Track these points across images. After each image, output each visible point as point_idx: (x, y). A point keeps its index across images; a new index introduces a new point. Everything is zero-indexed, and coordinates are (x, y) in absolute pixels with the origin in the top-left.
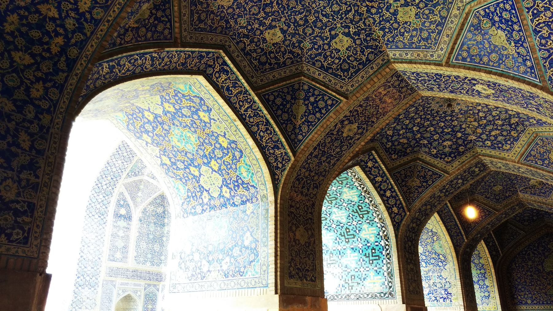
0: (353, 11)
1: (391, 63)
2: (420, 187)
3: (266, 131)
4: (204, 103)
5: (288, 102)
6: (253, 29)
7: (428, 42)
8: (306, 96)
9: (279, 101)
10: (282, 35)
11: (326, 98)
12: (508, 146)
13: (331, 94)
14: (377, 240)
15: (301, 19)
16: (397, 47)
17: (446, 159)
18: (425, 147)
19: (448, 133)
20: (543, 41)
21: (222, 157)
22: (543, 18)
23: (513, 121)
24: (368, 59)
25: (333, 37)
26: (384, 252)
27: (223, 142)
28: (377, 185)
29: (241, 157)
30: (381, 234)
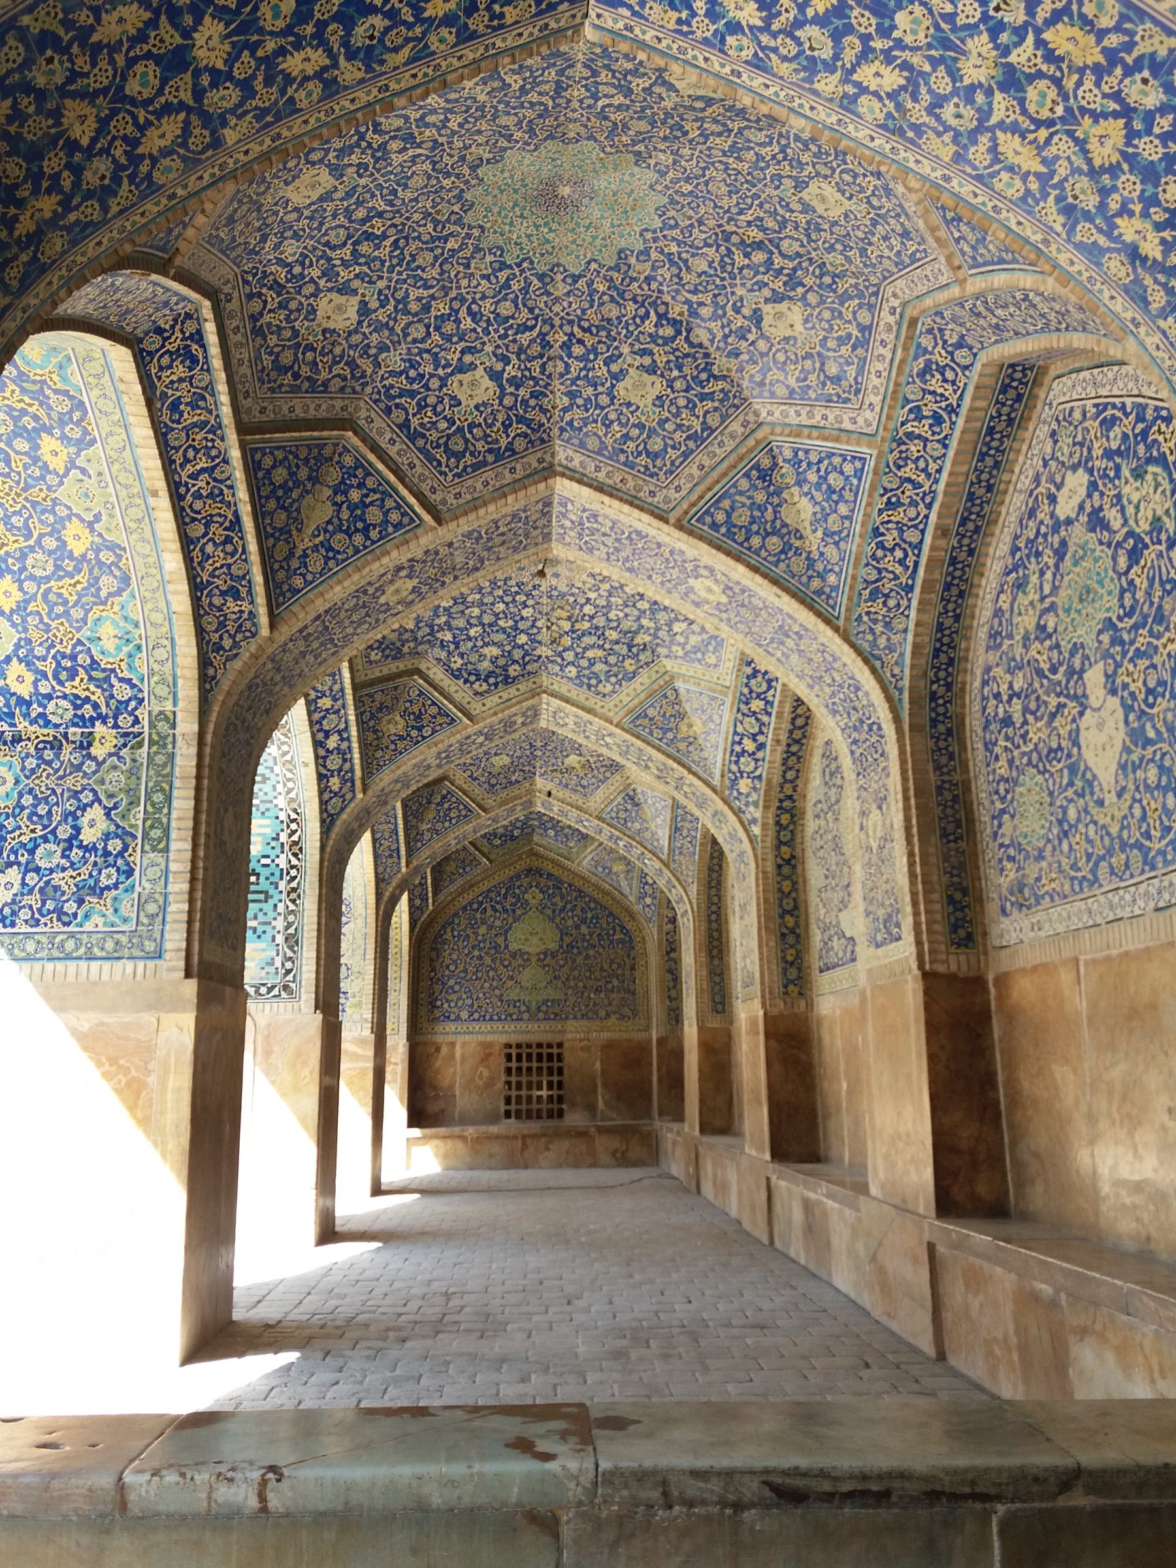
0: (535, 333)
1: (555, 474)
2: (401, 738)
3: (224, 543)
4: (81, 420)
5: (298, 483)
6: (302, 276)
7: (654, 464)
8: (343, 482)
9: (280, 475)
10: (354, 317)
11: (389, 503)
13: (403, 499)
14: (268, 851)
15: (419, 299)
16: (582, 445)
17: (476, 686)
18: (442, 646)
19: (504, 630)
20: (880, 553)
21: (48, 579)
22: (899, 515)
23: (639, 640)
24: (510, 448)
25: (461, 369)
26: (282, 885)
27: (77, 537)
28: (316, 716)
29: (119, 592)
30: (283, 837)
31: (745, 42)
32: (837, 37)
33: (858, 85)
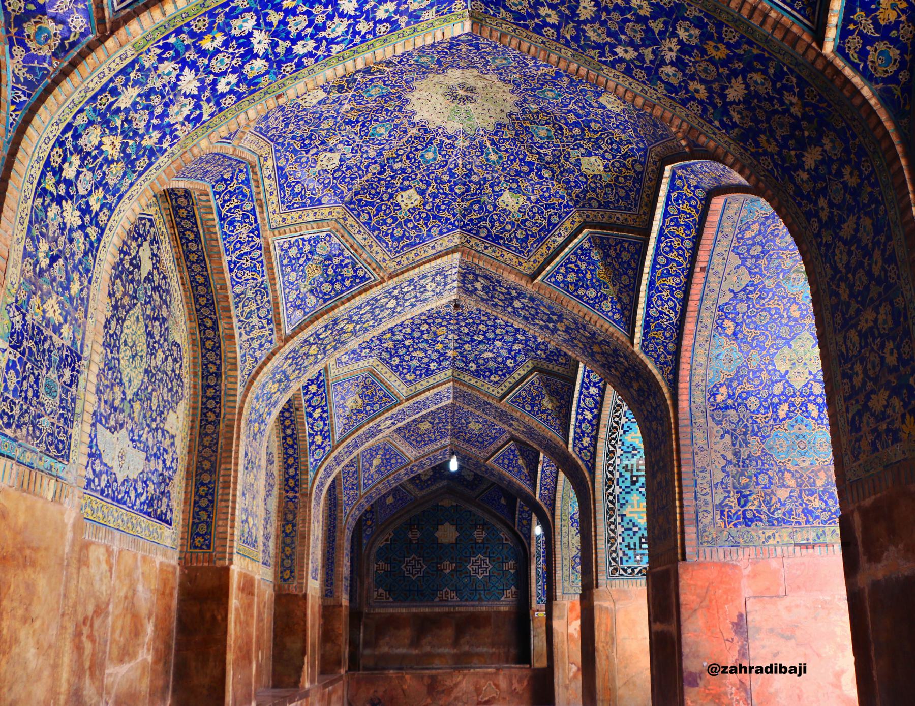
12: (498, 378)
19: (427, 341)
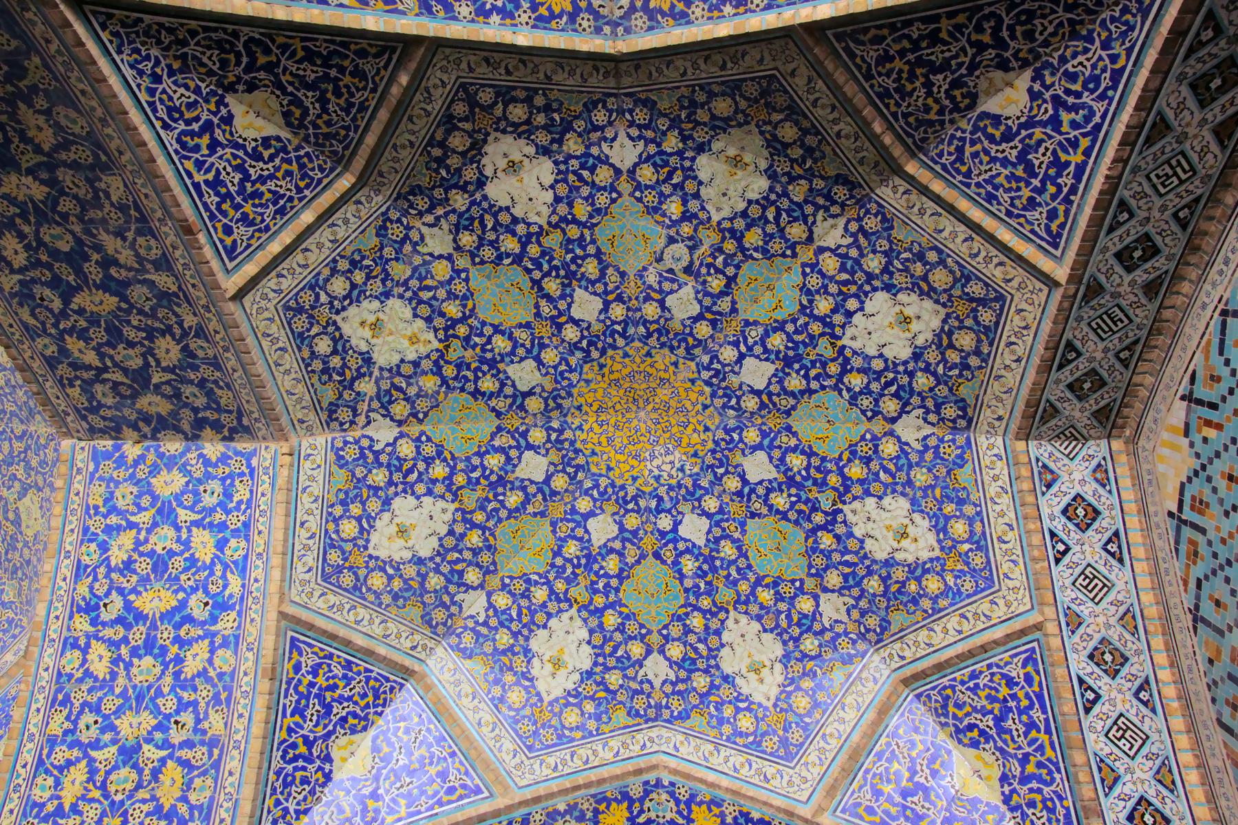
31: (96, 557)
32: (120, 620)
33: (88, 645)
